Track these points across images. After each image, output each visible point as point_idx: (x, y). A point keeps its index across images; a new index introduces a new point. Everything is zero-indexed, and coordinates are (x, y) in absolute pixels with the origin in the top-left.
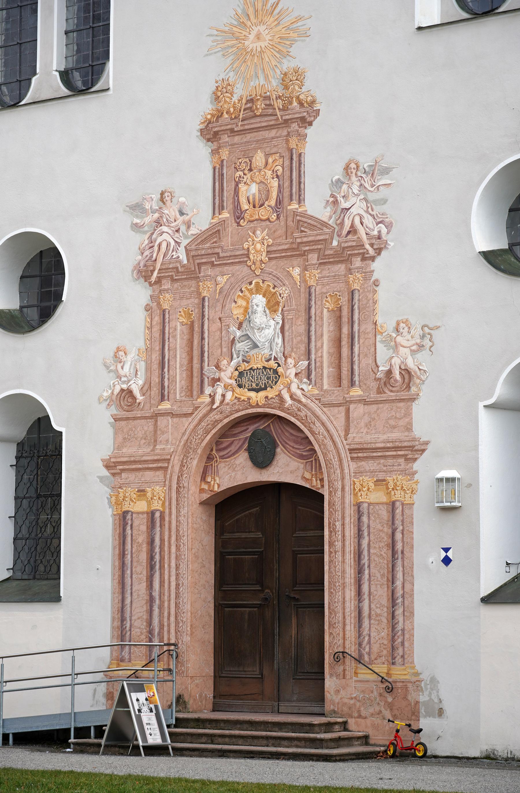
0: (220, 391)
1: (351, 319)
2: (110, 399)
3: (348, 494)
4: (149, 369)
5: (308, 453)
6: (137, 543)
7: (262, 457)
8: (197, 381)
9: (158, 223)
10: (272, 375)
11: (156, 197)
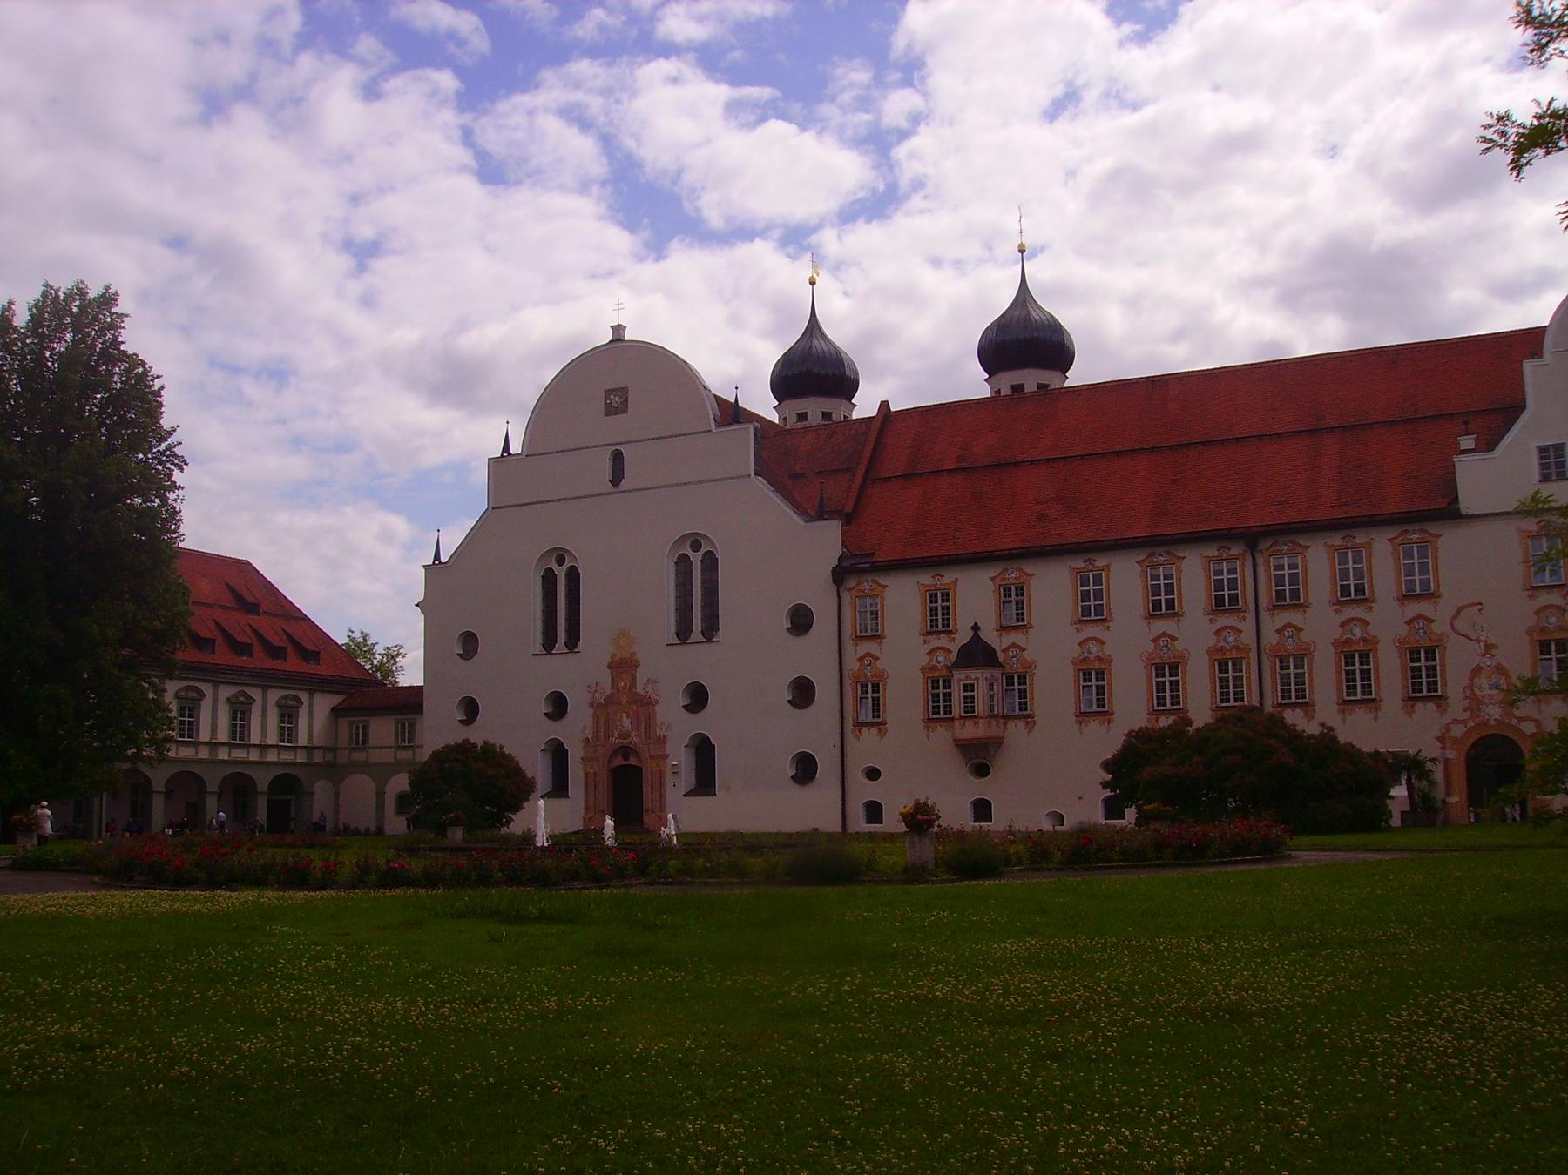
6: (590, 781)
7: (626, 759)
8: (607, 737)
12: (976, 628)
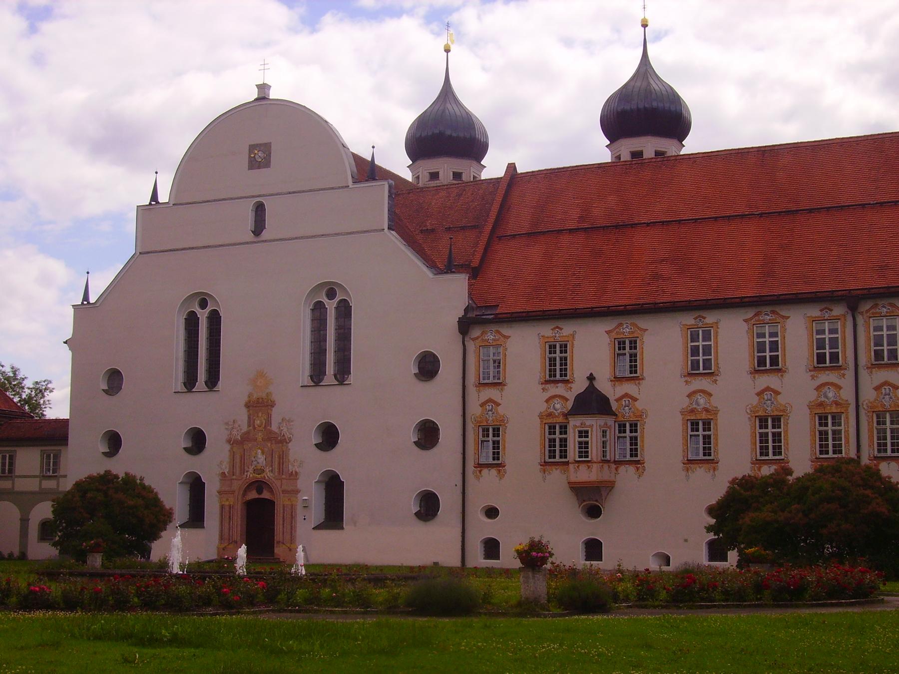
1: (283, 458)
3: (281, 502)
5: (271, 490)
7: (260, 491)
8: (243, 471)
12: (591, 378)
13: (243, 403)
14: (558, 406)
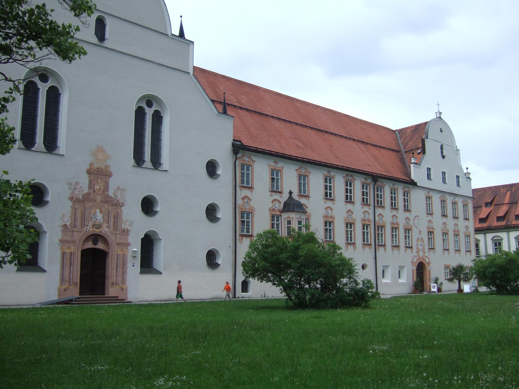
0: (88, 228)
1: (117, 218)
2: (61, 226)
3: (114, 252)
4: (71, 220)
8: (83, 225)
9: (75, 189)
10: (100, 226)
11: (75, 183)
12: (291, 193)
13: (85, 170)
14: (277, 205)
